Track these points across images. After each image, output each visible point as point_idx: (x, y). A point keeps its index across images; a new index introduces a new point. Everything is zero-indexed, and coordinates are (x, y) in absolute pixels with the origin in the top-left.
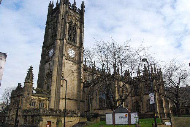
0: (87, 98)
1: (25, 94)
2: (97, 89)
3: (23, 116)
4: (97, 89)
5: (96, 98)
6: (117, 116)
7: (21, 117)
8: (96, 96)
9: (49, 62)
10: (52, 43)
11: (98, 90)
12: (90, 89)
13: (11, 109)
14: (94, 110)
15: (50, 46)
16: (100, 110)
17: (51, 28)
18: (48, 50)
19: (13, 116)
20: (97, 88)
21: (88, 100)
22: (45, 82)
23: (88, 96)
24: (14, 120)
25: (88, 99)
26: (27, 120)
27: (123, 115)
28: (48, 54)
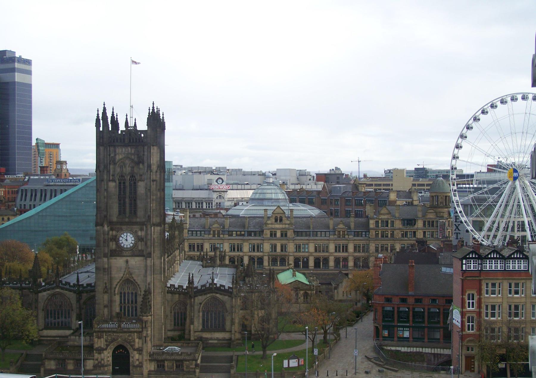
0: (171, 309)
1: (148, 333)
2: (201, 304)
3: (149, 360)
4: (201, 304)
5: (199, 316)
6: (291, 361)
7: (148, 361)
8: (199, 312)
9: (125, 258)
10: (127, 220)
11: (202, 305)
12: (178, 297)
13: (106, 349)
14: (195, 332)
15: (122, 223)
16: (205, 333)
17: (114, 180)
18: (112, 229)
19: (108, 359)
20: (201, 302)
21: (173, 314)
22: (116, 292)
23: (174, 308)
24: (111, 364)
25: (173, 312)
26: (166, 364)
27: (295, 360)
28: (115, 239)
